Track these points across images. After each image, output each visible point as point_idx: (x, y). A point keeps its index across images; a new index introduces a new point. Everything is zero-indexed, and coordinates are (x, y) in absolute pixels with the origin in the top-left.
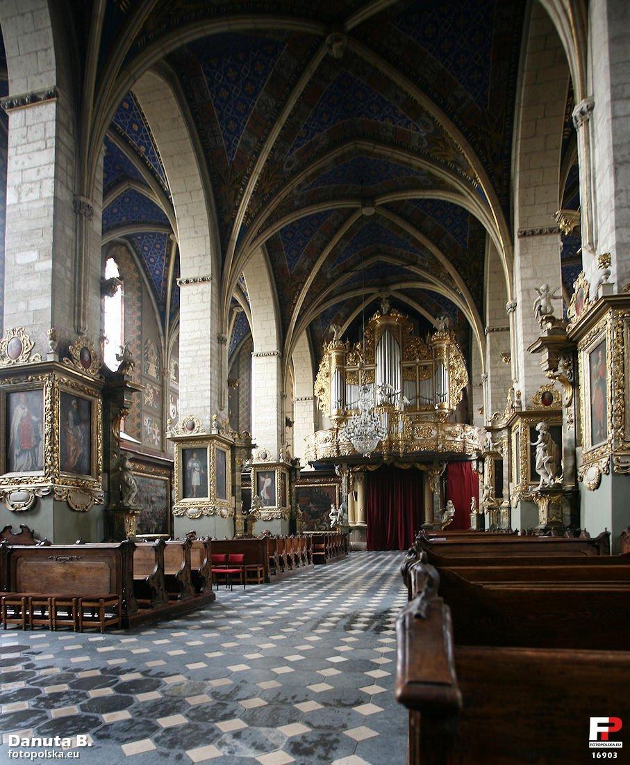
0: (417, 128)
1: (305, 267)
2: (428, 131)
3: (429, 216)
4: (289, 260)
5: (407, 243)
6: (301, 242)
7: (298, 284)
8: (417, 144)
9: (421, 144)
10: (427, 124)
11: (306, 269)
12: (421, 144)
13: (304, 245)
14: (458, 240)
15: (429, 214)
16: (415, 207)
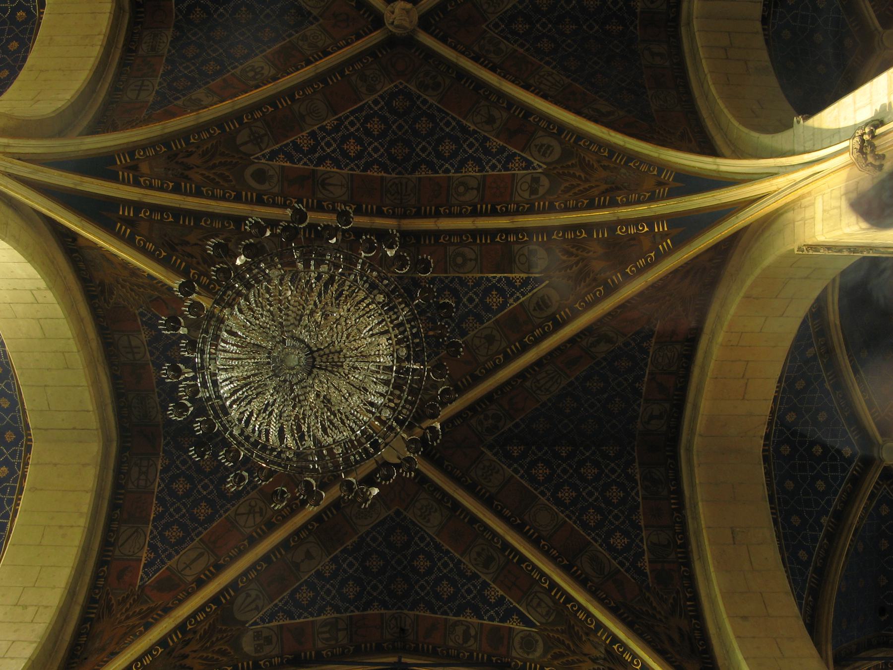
0: (527, 161)
1: (190, 576)
2: (549, 160)
3: (543, 499)
4: (153, 548)
5: (485, 585)
6: (203, 511)
7: (152, 610)
8: (526, 195)
9: (534, 191)
10: (549, 146)
11: (190, 579)
12: (534, 191)
13: (210, 519)
14: (622, 564)
15: (543, 494)
16: (510, 471)
